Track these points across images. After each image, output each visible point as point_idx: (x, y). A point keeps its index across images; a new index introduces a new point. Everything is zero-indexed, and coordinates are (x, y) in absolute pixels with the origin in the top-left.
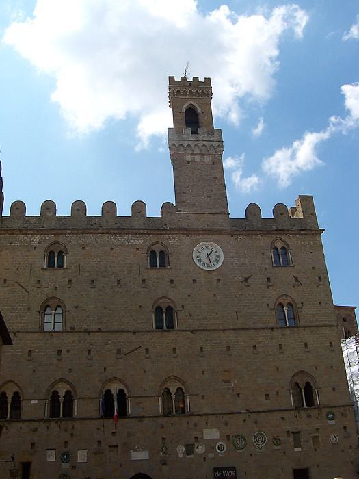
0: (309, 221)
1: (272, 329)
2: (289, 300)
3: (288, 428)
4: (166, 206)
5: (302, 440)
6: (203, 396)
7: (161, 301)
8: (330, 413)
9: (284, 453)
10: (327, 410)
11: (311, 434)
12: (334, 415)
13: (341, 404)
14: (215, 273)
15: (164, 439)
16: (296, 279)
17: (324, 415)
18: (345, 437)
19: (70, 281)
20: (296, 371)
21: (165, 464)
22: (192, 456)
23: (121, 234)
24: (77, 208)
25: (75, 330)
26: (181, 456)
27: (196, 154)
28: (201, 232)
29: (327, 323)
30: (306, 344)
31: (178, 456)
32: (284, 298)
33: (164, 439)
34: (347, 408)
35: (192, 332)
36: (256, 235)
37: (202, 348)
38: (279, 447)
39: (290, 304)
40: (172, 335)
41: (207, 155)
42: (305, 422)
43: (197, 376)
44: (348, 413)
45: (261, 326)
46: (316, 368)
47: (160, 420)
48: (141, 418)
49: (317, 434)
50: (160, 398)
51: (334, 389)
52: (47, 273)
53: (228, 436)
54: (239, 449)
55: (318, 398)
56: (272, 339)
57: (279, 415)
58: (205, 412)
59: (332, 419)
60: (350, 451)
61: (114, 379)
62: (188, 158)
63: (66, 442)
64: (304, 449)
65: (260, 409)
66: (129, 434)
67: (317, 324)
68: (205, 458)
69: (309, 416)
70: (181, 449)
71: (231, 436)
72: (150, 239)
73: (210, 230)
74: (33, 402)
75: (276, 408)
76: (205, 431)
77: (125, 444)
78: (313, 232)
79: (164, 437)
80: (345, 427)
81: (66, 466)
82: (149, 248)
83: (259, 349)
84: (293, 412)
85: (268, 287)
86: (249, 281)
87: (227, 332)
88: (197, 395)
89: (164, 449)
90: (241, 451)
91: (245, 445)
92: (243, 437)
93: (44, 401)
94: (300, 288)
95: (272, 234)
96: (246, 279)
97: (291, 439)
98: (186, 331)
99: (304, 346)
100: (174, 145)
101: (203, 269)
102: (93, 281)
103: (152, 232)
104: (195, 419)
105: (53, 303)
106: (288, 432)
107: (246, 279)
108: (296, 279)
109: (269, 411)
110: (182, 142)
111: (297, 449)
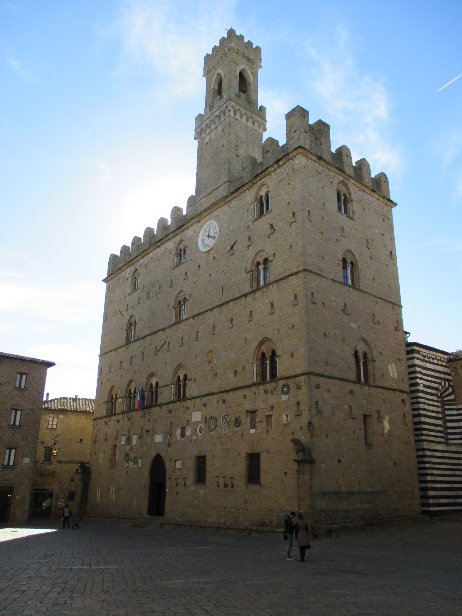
0: (291, 143)
1: (246, 295)
2: (265, 255)
3: (248, 406)
4: (192, 201)
5: (257, 421)
6: (195, 380)
7: (181, 295)
8: (284, 386)
9: (242, 434)
10: (282, 383)
11: (265, 413)
12: (288, 388)
13: (298, 373)
14: (212, 252)
15: (171, 423)
16: (272, 226)
17: (280, 388)
18: (296, 415)
19: (139, 298)
20: (261, 339)
21: (170, 446)
22: (183, 439)
23: (162, 244)
24: (145, 234)
25: (139, 337)
26: (178, 438)
27: (213, 130)
28: (205, 214)
29: (295, 270)
30: (272, 304)
31: (177, 438)
32: (261, 254)
33: (171, 423)
34: (303, 378)
35: (193, 317)
36: (244, 192)
37: (198, 332)
38: (238, 429)
39: (266, 261)
40: (181, 325)
41: (219, 125)
42: (261, 400)
43: (192, 361)
44: (303, 384)
45: (237, 295)
46: (278, 331)
47: (171, 406)
48: (161, 405)
49: (270, 413)
50: (173, 386)
51: (292, 354)
52: (130, 297)
53: (206, 417)
54: (212, 431)
55: (281, 370)
56: (245, 307)
57: (241, 393)
58: (193, 396)
59: (287, 393)
60: (300, 433)
61: (152, 375)
62: (207, 140)
63: (130, 429)
64: (258, 431)
65: (229, 388)
66: (155, 420)
67: (286, 274)
68: (191, 440)
69: (266, 392)
70: (179, 431)
71: (208, 418)
72: (177, 239)
73: (209, 208)
74: (120, 400)
75: (240, 385)
76: (194, 414)
77: (153, 428)
78: (291, 156)
79: (172, 421)
80: (298, 403)
81: (128, 447)
82: (177, 248)
83: (234, 322)
84: (254, 388)
85: (248, 247)
86: (235, 248)
87: (214, 310)
88: (191, 379)
89: (170, 432)
90: (213, 433)
91: (216, 427)
92: (215, 419)
93: (123, 399)
94: (273, 237)
95: (256, 183)
96: (232, 247)
97: (249, 419)
98: (188, 319)
99: (270, 307)
100: (198, 132)
101: (204, 252)
102: (148, 293)
103: (177, 233)
104: (188, 403)
105: (132, 320)
106: (247, 411)
107: (232, 247)
108: (272, 226)
109: (235, 389)
110: (202, 127)
111: (253, 431)
